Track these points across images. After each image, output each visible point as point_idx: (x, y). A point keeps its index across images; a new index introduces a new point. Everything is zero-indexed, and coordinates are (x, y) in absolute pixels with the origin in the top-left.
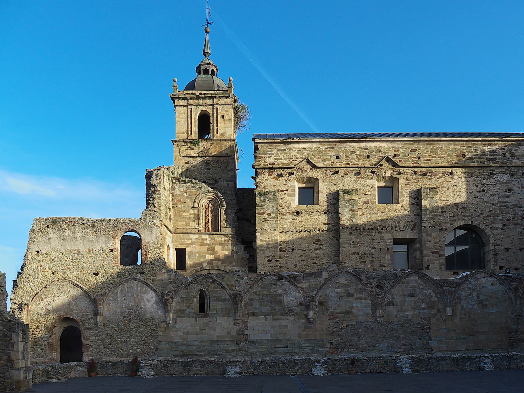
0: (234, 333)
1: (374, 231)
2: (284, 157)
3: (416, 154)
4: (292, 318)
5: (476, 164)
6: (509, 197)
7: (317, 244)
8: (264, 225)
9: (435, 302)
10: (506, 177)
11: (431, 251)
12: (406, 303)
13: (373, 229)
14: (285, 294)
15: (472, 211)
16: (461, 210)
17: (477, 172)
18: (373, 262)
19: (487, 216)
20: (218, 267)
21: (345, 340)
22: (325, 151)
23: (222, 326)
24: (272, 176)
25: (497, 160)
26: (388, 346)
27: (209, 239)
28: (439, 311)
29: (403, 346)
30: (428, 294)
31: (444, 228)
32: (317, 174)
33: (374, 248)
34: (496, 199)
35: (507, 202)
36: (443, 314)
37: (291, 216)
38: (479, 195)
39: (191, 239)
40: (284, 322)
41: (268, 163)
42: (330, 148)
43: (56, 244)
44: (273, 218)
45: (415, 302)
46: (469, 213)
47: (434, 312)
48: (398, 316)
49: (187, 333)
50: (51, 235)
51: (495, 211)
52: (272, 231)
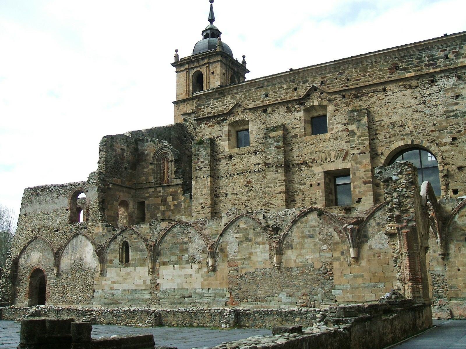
0: (148, 283)
1: (303, 166)
2: (219, 104)
4: (195, 266)
5: (412, 74)
6: (458, 103)
8: (198, 173)
10: (452, 81)
11: (362, 181)
13: (302, 164)
14: (190, 242)
15: (412, 128)
16: (399, 129)
17: (414, 83)
18: (303, 199)
19: (432, 131)
20: (169, 217)
21: (243, 290)
22: (255, 92)
23: (140, 275)
24: (208, 125)
25: (438, 64)
26: (287, 296)
27: (162, 191)
28: (342, 253)
29: (303, 295)
30: (329, 234)
31: (379, 152)
33: (304, 184)
34: (441, 109)
35: (456, 110)
36: (347, 257)
37: (224, 161)
38: (419, 108)
39: (149, 193)
40: (189, 271)
41: (206, 113)
46: (408, 131)
47: (337, 254)
48: (297, 261)
49: (114, 282)
51: (441, 124)
52: (206, 178)
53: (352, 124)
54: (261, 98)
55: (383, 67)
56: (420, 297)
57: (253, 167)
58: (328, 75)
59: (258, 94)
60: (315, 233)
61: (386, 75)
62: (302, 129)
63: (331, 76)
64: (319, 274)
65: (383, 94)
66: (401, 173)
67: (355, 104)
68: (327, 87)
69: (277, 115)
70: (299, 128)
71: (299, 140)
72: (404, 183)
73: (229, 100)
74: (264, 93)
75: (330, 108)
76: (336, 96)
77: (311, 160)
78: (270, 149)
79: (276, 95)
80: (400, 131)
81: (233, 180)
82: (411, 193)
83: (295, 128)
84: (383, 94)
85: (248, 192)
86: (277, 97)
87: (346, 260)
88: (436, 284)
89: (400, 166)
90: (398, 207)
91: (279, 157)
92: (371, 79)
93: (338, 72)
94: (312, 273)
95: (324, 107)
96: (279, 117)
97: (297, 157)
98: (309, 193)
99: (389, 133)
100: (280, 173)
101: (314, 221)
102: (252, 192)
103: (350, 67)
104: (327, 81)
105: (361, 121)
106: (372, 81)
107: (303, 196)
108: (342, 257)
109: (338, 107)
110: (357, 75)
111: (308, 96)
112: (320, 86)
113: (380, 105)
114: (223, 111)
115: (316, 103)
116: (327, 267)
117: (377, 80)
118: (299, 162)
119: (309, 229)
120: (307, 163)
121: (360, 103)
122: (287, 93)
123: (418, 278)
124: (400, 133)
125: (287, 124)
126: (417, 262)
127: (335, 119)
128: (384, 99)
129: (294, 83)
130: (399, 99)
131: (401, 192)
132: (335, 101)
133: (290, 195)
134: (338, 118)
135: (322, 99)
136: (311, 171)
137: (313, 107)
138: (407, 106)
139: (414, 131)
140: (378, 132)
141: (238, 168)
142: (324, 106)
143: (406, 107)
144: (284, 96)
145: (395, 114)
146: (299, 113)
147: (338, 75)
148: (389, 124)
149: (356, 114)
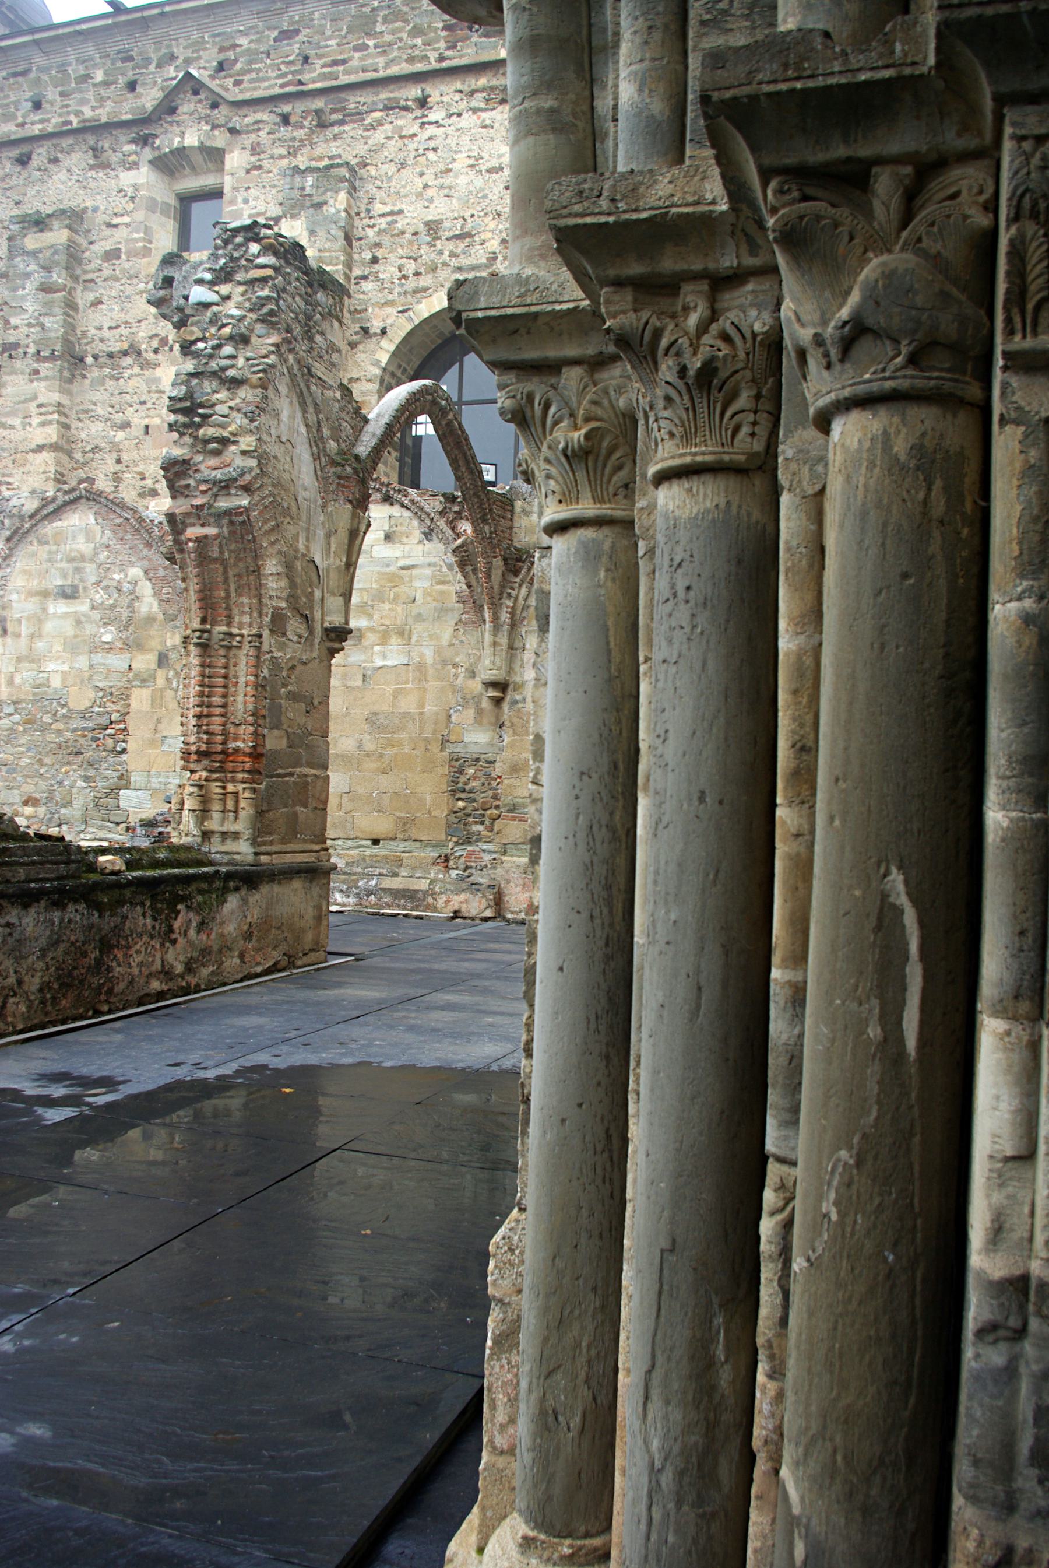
1: (128, 361)
3: (294, 48)
9: (150, 619)
12: (49, 626)
13: (125, 353)
16: (451, 245)
29: (25, 803)
30: (126, 587)
31: (376, 326)
33: (126, 425)
42: (15, 75)
45: (78, 622)
47: (144, 662)
48: (17, 680)
53: (293, 216)
54: (19, 114)
55: (426, 20)
56: (236, 835)
58: (243, 41)
59: (8, 97)
60: (82, 580)
61: (434, 50)
62: (137, 232)
63: (252, 46)
64: (84, 729)
65: (416, 118)
66: (224, 275)
67: (319, 151)
68: (237, 83)
69: (63, 175)
70: (127, 225)
71: (123, 270)
72: (232, 317)
74: (28, 94)
75: (236, 160)
76: (259, 116)
77: (155, 343)
78: (20, 292)
79: (67, 106)
80: (453, 255)
82: (253, 366)
83: (116, 226)
84: (416, 118)
86: (68, 113)
87: (175, 684)
88: (464, 791)
89: (226, 242)
90: (185, 426)
91: (48, 322)
92: (381, 61)
93: (275, 28)
94: (61, 726)
95: (215, 156)
97: (110, 328)
98: (137, 458)
99: (415, 260)
100: (46, 378)
101: (81, 539)
103: (317, 15)
104: (236, 61)
105: (325, 208)
106: (385, 68)
107: (118, 467)
108: (161, 675)
109: (262, 156)
110: (338, 45)
111: (168, 108)
112: (212, 77)
113: (401, 156)
115: (191, 140)
116: (111, 707)
117: (404, 65)
118: (117, 347)
119: (64, 565)
120: (139, 353)
121: (334, 148)
122: (102, 100)
123: (237, 750)
124: (454, 262)
125: (90, 211)
126: (242, 680)
127: (246, 201)
128: (415, 135)
129: (130, 64)
130: (468, 138)
131: (211, 356)
132: (253, 136)
133: (77, 462)
134: (257, 198)
135: (214, 127)
136: (150, 381)
137: (181, 152)
138: (489, 165)
139: (500, 258)
140: (379, 254)
142: (217, 149)
143: (483, 168)
144: (93, 109)
145: (446, 191)
146: (133, 172)
147: (275, 40)
148: (421, 228)
149: (310, 181)
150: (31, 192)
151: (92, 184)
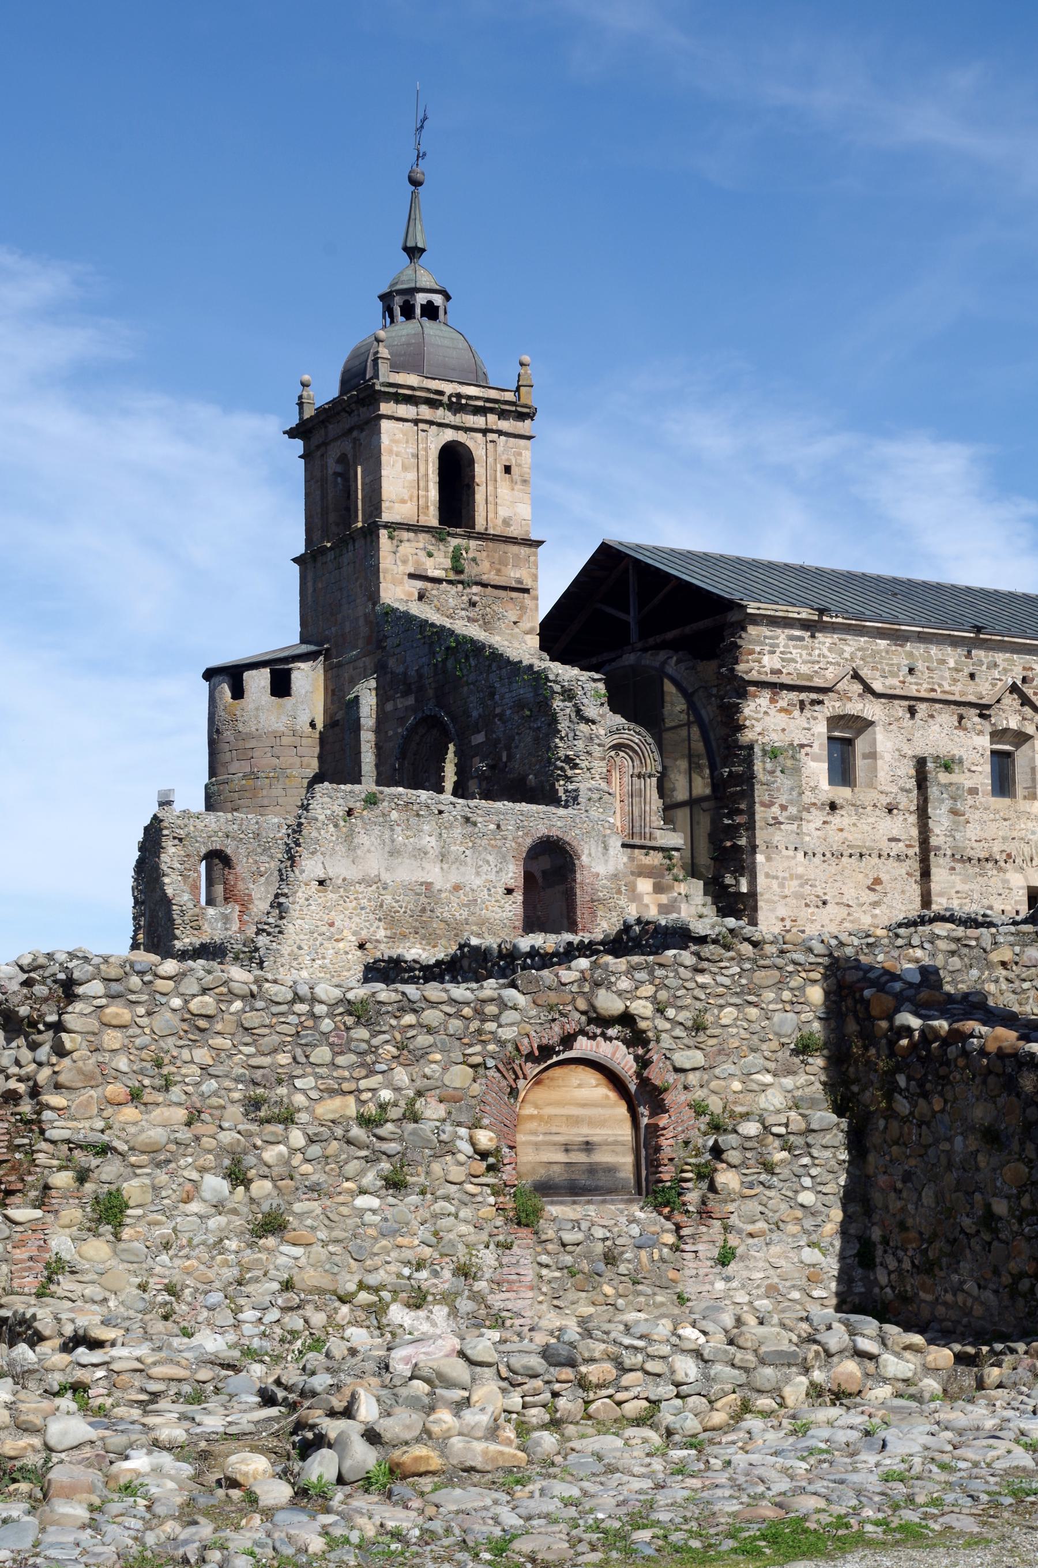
1: (990, 865)
7: (873, 890)
8: (773, 834)
13: (987, 860)
32: (871, 709)
43: (374, 863)
44: (792, 819)
50: (362, 839)
57: (885, 846)
73: (826, 652)
74: (906, 662)
81: (840, 867)
85: (875, 904)
96: (937, 735)
102: (884, 907)
114: (810, 678)
135: (1024, 719)
141: (850, 838)
150: (918, 734)
151: (956, 739)
